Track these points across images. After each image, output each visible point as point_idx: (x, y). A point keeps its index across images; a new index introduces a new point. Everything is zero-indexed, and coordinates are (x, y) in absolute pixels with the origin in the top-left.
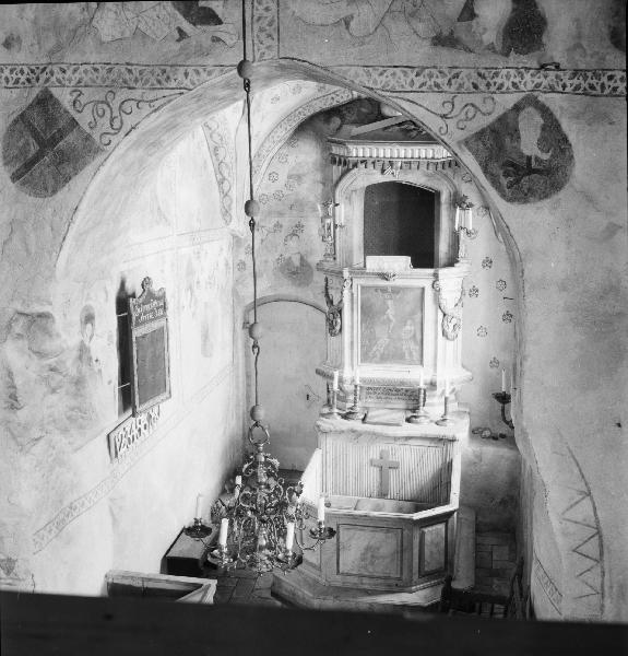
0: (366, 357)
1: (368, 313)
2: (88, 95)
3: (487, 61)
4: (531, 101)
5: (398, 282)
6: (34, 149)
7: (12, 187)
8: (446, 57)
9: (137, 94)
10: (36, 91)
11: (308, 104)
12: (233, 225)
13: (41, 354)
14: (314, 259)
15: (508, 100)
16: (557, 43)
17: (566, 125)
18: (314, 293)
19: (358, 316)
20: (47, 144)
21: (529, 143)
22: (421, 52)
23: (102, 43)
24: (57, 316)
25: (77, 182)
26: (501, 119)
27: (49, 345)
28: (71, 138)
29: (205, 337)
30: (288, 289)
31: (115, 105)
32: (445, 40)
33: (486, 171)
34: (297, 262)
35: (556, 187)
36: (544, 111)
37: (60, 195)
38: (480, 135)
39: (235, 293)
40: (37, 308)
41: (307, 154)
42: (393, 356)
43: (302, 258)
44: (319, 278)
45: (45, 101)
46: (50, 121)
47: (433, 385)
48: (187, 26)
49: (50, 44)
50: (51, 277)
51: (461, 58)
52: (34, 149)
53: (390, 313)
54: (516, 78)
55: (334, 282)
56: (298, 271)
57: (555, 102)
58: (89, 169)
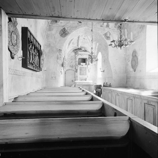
0: (80, 75)
1: (80, 70)
2: (69, 28)
3: (105, 28)
6: (63, 33)
7: (60, 36)
10: (64, 27)
13: (60, 55)
14: (73, 66)
15: (106, 32)
18: (74, 69)
20: (64, 33)
21: (108, 35)
22: (99, 27)
23: (70, 24)
25: (67, 37)
28: (67, 32)
30: (70, 68)
32: (102, 26)
33: (105, 37)
34: (72, 65)
37: (65, 37)
40: (61, 49)
41: (73, 54)
43: (72, 65)
44: (74, 67)
45: (64, 29)
46: (64, 30)
47: (88, 77)
48: (79, 23)
49: (65, 23)
50: (63, 46)
52: (63, 33)
53: (83, 70)
54: (107, 30)
55: (76, 67)
56: (72, 67)
58: (68, 35)
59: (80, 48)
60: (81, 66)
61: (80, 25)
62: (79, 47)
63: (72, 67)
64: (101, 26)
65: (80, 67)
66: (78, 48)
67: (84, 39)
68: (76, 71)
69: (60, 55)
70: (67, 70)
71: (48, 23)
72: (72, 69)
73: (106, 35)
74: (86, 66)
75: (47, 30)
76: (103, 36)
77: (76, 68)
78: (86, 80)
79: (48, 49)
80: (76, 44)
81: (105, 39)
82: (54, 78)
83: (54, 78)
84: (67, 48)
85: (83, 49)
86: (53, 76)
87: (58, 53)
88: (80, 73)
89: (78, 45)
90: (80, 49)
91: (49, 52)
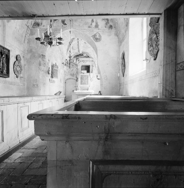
0: (81, 84)
1: (81, 78)
4: (98, 33)
5: (85, 74)
8: (89, 28)
9: (58, 31)
11: (74, 55)
12: (64, 69)
13: (44, 61)
14: (75, 74)
15: (95, 33)
16: (100, 27)
17: (101, 35)
19: (80, 79)
22: (87, 28)
24: (46, 56)
26: (95, 34)
27: (45, 60)
29: (61, 80)
31: (55, 32)
32: (90, 27)
35: (100, 40)
36: (99, 33)
38: (93, 36)
39: (64, 78)
40: (44, 54)
42: (85, 84)
44: (75, 76)
48: (63, 25)
50: (46, 51)
51: (91, 29)
54: (96, 31)
56: (73, 75)
57: (100, 33)
59: (82, 54)
60: (82, 74)
61: (65, 28)
62: (81, 53)
63: (73, 75)
64: (88, 27)
65: (81, 76)
66: (79, 54)
67: (85, 43)
68: (77, 80)
69: (44, 61)
70: (67, 79)
71: (28, 27)
72: (72, 78)
73: (94, 36)
74: (88, 74)
75: (28, 35)
76: (92, 38)
77: (77, 77)
78: (88, 90)
79: (29, 55)
80: (77, 50)
81: (94, 41)
82: (36, 86)
83: (36, 86)
84: (65, 55)
85: (85, 55)
86: (34, 84)
87: (40, 59)
88: (81, 82)
89: (79, 51)
90: (81, 55)
91: (30, 58)
